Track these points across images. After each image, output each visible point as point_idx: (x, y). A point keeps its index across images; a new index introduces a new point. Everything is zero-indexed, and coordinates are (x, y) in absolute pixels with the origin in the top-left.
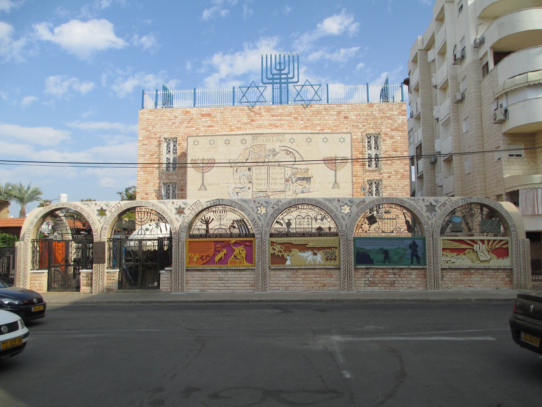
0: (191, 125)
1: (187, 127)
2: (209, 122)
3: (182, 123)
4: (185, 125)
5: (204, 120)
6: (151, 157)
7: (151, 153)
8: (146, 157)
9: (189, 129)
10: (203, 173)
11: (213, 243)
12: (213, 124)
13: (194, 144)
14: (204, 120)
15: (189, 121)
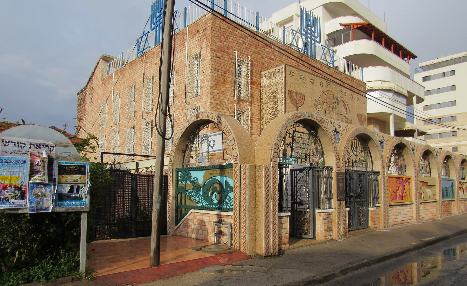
0: (257, 50)
1: (255, 52)
2: (271, 54)
3: (250, 45)
4: (253, 49)
5: (267, 50)
6: (224, 74)
7: (224, 70)
8: (220, 74)
9: (257, 55)
10: (297, 107)
11: (395, 179)
12: (273, 57)
13: (290, 74)
14: (267, 50)
15: (257, 47)
